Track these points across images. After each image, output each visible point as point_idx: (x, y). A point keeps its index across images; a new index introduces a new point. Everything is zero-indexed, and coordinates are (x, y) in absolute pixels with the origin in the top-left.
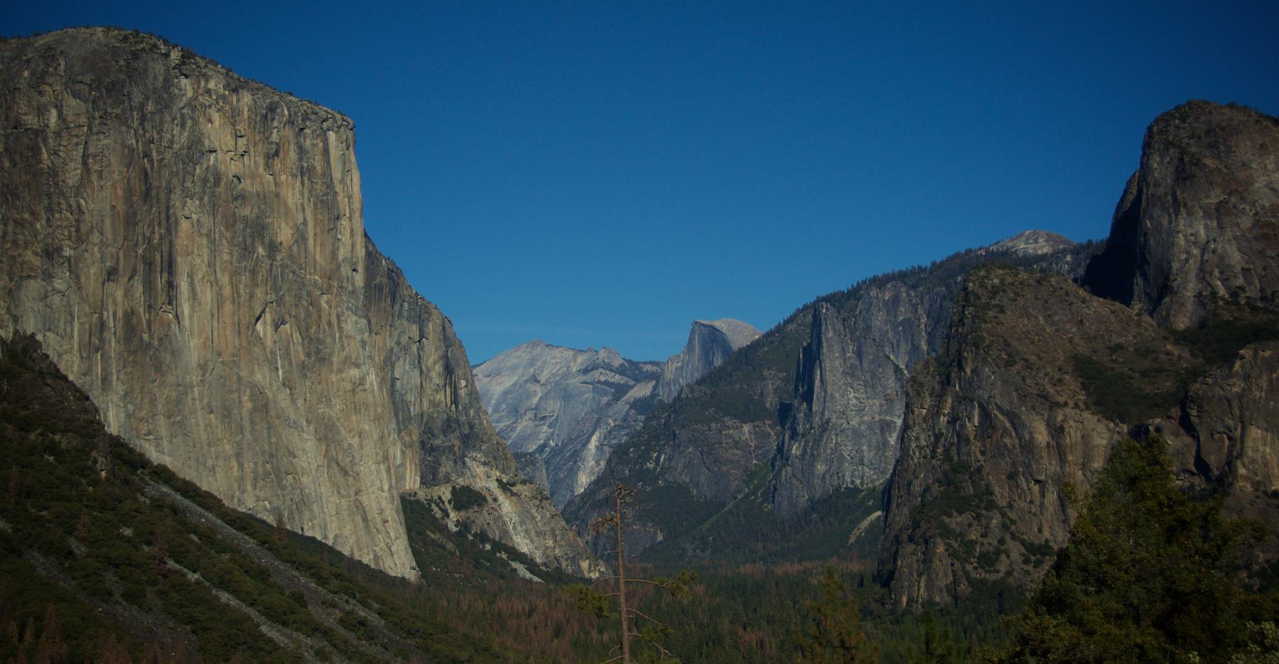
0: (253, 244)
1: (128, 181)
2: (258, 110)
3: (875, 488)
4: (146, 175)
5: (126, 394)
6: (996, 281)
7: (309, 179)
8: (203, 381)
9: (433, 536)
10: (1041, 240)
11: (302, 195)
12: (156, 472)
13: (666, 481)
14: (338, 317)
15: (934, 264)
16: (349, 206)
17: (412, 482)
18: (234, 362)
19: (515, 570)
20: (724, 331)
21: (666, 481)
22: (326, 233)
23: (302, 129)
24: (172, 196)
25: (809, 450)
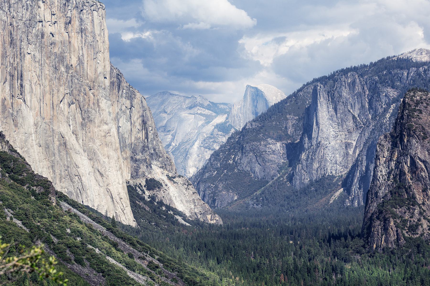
0: (59, 66)
1: (3, 37)
2: (62, 2)
3: (342, 176)
4: (11, 33)
6: (418, 98)
7: (85, 34)
8: (36, 131)
9: (138, 203)
10: (423, 53)
12: (61, 197)
13: (238, 170)
15: (371, 63)
16: (103, 47)
17: (128, 177)
18: (50, 122)
19: (177, 220)
20: (262, 90)
21: (238, 170)
22: (92, 60)
23: (82, 10)
24: (22, 43)
25: (310, 157)
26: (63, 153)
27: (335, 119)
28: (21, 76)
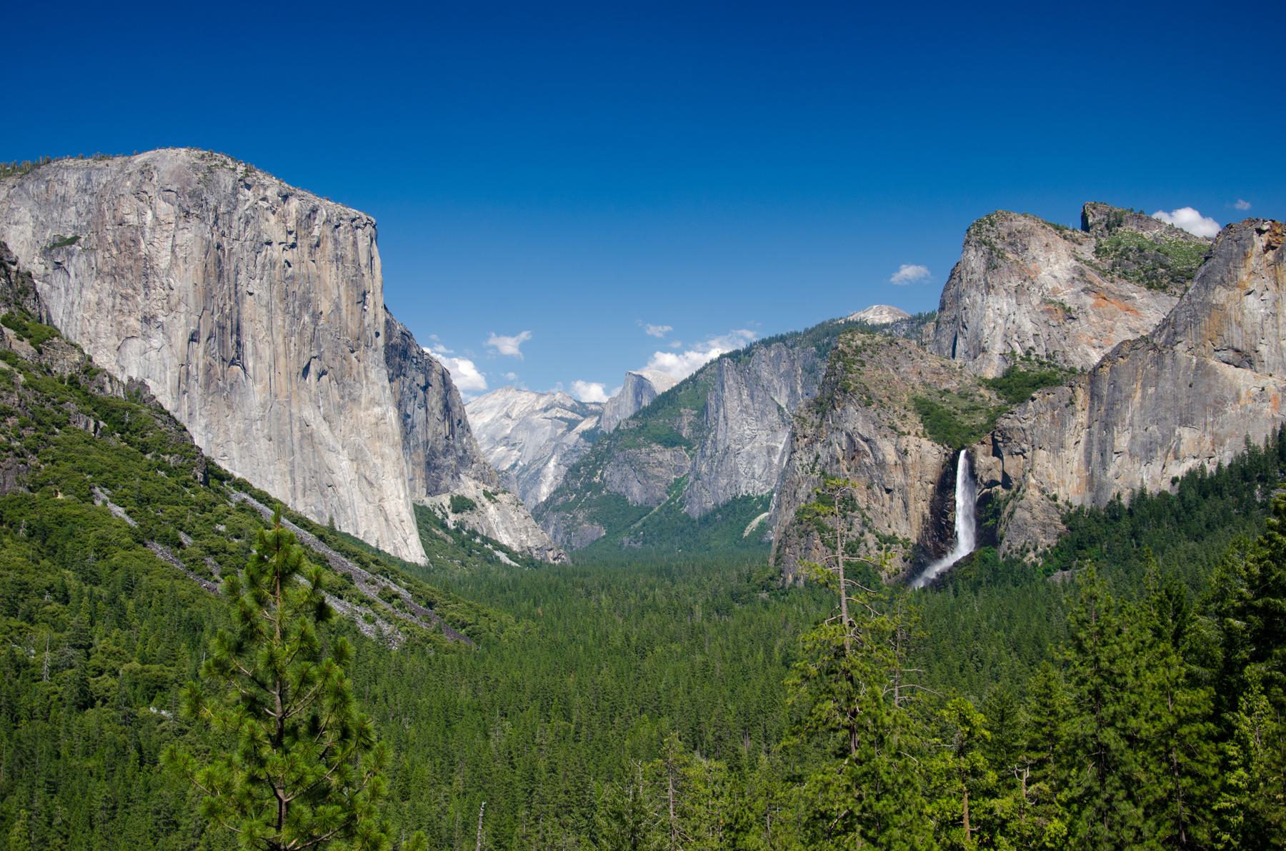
0: (300, 313)
4: (220, 261)
5: (206, 426)
6: (859, 343)
10: (884, 313)
11: (337, 275)
13: (608, 491)
14: (365, 368)
15: (806, 330)
21: (608, 491)
23: (337, 227)
26: (308, 450)
27: (751, 411)
28: (238, 329)
